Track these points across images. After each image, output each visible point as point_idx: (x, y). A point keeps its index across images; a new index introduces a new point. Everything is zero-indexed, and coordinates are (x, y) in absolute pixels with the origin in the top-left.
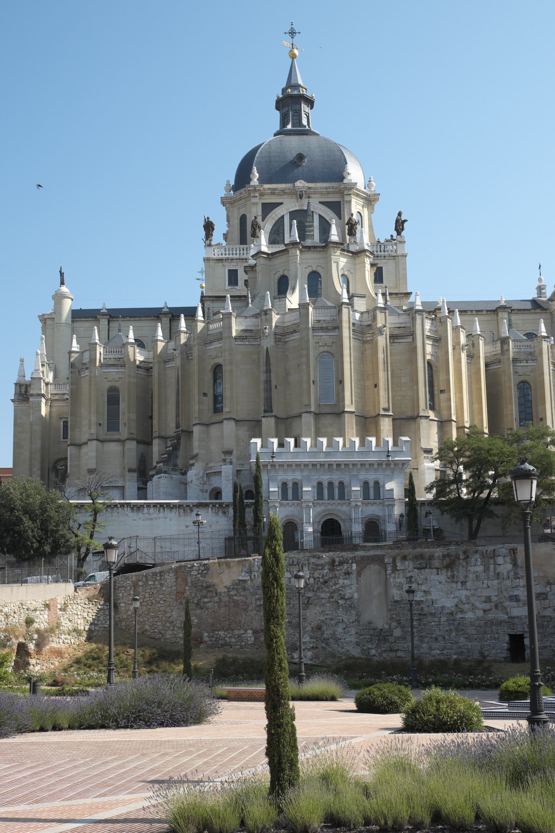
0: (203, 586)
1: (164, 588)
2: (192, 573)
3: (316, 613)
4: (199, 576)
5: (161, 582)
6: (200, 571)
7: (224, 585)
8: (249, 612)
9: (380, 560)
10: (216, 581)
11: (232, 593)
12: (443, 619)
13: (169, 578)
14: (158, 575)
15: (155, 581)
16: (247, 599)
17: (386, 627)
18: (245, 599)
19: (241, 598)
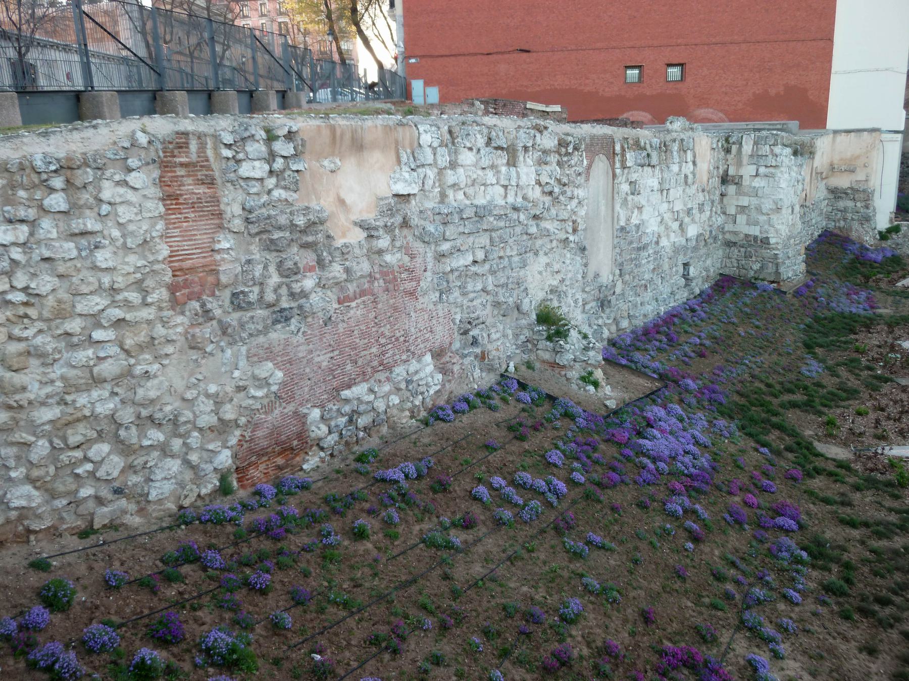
0: (293, 226)
1: (103, 257)
2: (245, 170)
3: (540, 273)
4: (271, 182)
5: (77, 225)
6: (279, 164)
7: (355, 217)
8: (421, 300)
9: (607, 148)
10: (324, 203)
11: (384, 242)
12: (651, 251)
13: (131, 196)
14: (58, 182)
15: (33, 224)
16: (412, 257)
17: (611, 278)
18: (407, 259)
19: (398, 255)
